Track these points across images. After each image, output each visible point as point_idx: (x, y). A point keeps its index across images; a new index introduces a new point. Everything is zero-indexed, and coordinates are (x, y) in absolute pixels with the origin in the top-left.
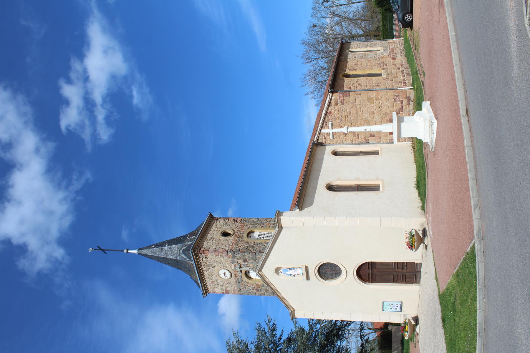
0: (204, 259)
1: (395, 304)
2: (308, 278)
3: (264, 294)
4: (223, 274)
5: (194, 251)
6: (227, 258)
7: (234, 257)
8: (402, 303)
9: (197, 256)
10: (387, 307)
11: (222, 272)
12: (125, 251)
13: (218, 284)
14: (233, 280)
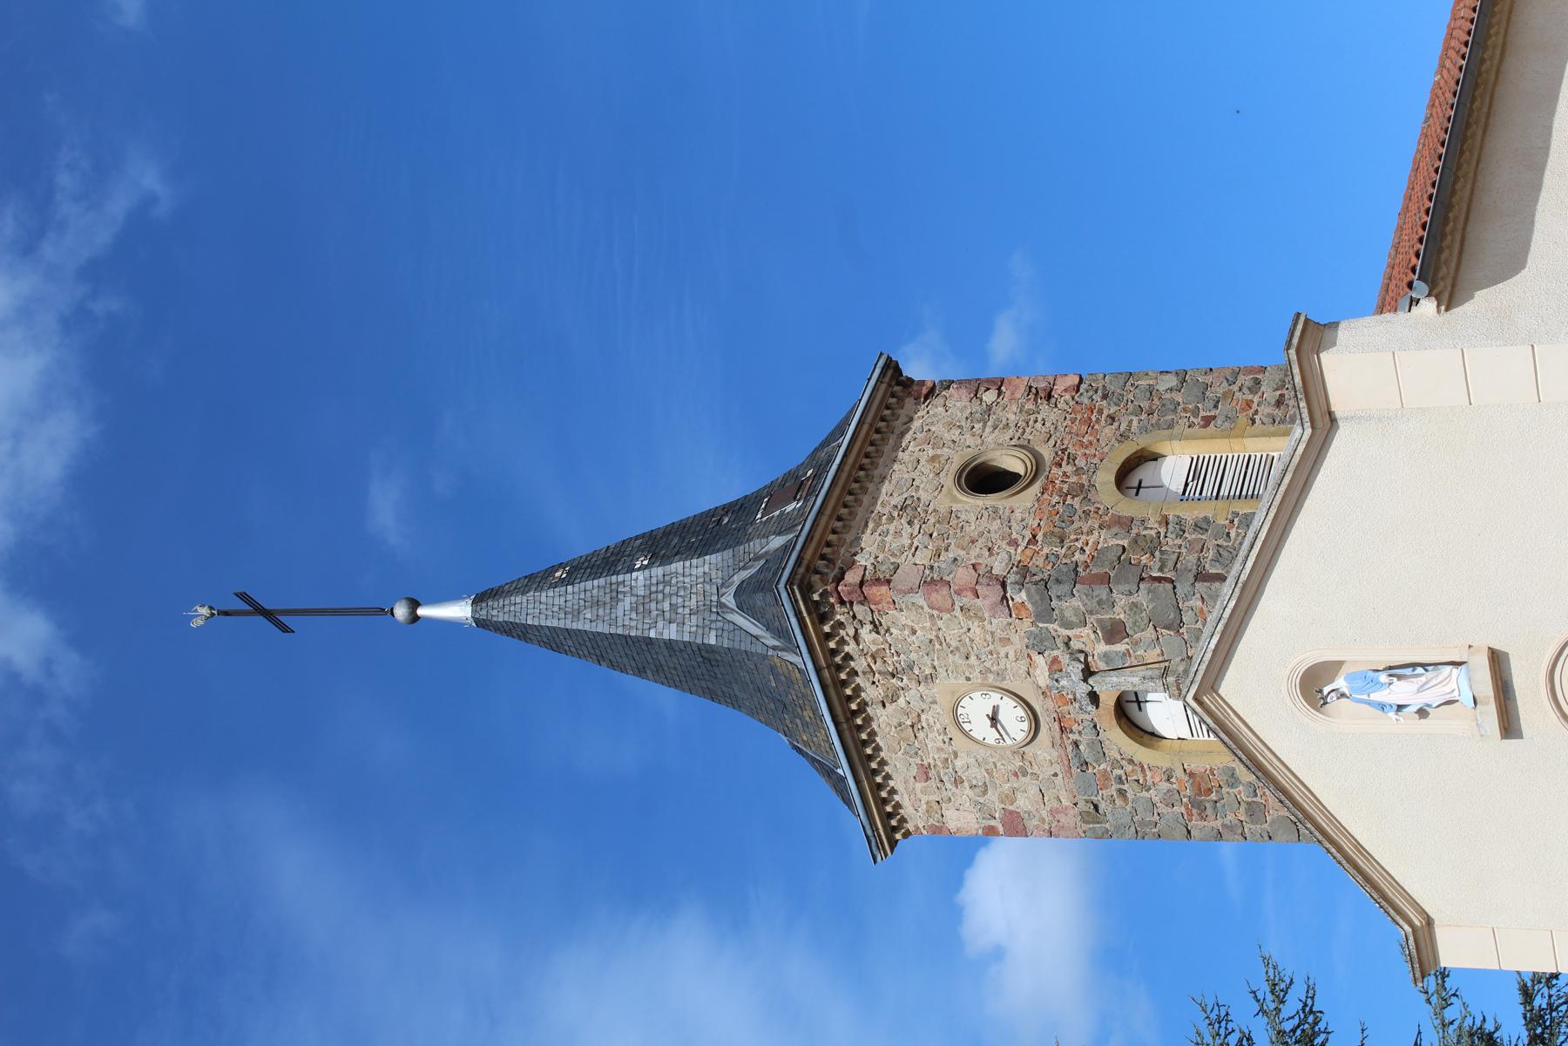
0: (866, 633)
2: (1509, 726)
4: (987, 717)
5: (807, 590)
6: (1000, 621)
7: (1045, 613)
9: (823, 618)
11: (975, 709)
12: (401, 612)
13: (958, 782)
14: (1044, 750)
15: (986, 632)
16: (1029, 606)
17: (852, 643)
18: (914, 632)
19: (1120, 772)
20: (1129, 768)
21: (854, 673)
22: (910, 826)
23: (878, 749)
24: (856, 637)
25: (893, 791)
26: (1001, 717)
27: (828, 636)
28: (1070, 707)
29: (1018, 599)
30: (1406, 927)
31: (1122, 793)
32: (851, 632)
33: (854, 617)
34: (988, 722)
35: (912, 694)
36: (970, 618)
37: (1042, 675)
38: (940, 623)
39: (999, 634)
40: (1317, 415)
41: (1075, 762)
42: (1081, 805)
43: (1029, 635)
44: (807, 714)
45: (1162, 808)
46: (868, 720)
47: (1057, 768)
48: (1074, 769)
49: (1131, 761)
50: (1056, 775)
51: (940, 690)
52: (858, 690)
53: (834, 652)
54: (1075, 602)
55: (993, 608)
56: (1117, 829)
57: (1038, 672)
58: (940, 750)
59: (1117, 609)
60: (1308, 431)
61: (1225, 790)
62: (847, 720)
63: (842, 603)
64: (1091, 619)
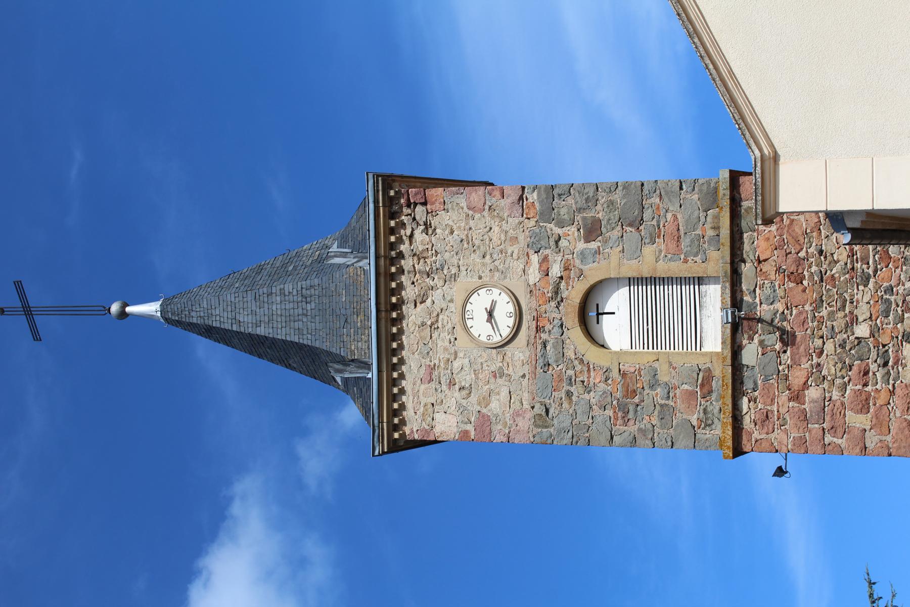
0: (419, 236)
3: (649, 434)
4: (488, 312)
5: (387, 186)
7: (548, 214)
9: (393, 215)
11: (479, 304)
12: (115, 308)
13: (452, 384)
14: (519, 352)
16: (537, 205)
17: (407, 242)
18: (452, 232)
19: (570, 372)
20: (579, 368)
21: (401, 271)
22: (407, 430)
23: (401, 347)
24: (411, 237)
25: (402, 391)
26: (495, 314)
27: (392, 231)
28: (547, 307)
29: (530, 200)
30: (757, 152)
31: (569, 394)
32: (408, 232)
33: (414, 219)
34: (486, 316)
35: (437, 295)
36: (493, 217)
37: (534, 275)
38: (471, 223)
41: (541, 362)
42: (537, 406)
43: (533, 235)
44: (361, 317)
45: (596, 411)
46: (401, 318)
47: (526, 369)
48: (539, 368)
49: (582, 361)
50: (524, 376)
51: (456, 291)
52: (400, 286)
53: (392, 246)
54: (570, 201)
55: (511, 208)
56: (559, 432)
57: (531, 270)
58: (446, 349)
59: (599, 207)
61: (647, 391)
62: (386, 311)
63: (409, 206)
64: (578, 218)
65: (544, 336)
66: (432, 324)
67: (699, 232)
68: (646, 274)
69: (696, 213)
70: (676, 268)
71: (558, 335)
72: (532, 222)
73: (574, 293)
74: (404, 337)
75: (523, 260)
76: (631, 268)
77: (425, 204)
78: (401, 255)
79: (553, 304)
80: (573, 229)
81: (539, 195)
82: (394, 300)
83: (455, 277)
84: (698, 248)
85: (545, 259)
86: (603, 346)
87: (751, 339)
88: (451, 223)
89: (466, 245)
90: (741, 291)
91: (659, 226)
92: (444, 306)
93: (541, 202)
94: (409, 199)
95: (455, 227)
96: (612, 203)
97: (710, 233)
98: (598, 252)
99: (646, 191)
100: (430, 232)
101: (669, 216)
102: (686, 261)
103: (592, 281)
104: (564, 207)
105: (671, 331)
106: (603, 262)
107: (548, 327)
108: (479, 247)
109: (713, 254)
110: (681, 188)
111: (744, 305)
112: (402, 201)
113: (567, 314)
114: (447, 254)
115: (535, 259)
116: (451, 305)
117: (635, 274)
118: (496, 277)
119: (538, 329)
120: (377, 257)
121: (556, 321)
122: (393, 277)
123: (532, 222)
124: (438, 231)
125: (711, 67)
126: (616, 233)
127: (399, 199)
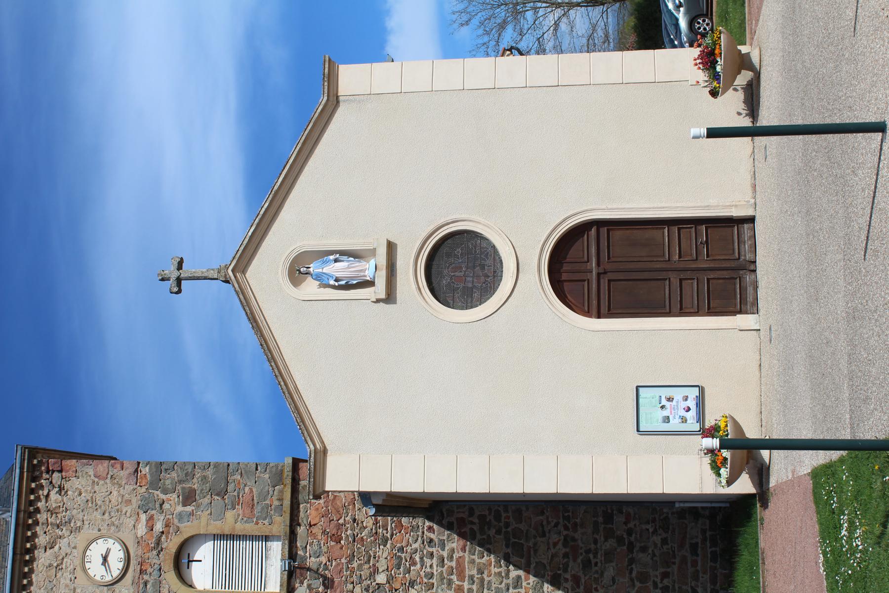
0: (54, 496)
1: (678, 394)
2: (390, 297)
4: (103, 558)
5: (32, 456)
7: (155, 484)
8: (702, 390)
9: (34, 479)
10: (652, 419)
11: (96, 550)
15: (120, 495)
16: (148, 476)
17: (44, 501)
18: (80, 494)
21: (36, 523)
24: (47, 496)
26: (109, 559)
27: (33, 491)
28: (150, 554)
29: (143, 472)
30: (312, 446)
32: (45, 493)
33: (51, 482)
35: (63, 543)
36: (114, 484)
37: (142, 530)
39: (127, 497)
40: (331, 94)
43: (143, 499)
46: (32, 560)
51: (80, 540)
52: (35, 535)
53: (31, 503)
54: (174, 474)
58: (67, 586)
59: (195, 480)
60: (326, 98)
63: (48, 472)
64: (179, 488)
65: (146, 577)
66: (58, 565)
67: (268, 502)
68: (227, 532)
69: (267, 488)
70: (250, 528)
71: (156, 577)
72: (144, 489)
73: (171, 545)
74: (33, 576)
75: (134, 518)
76: (216, 527)
77: (61, 471)
78: (38, 511)
79: (155, 552)
80: (175, 496)
81: (150, 469)
82: (28, 545)
83: (79, 529)
84: (266, 514)
85: (151, 518)
86: (191, 586)
87: (302, 583)
88: (80, 487)
89: (90, 505)
90: (296, 547)
91: (238, 496)
92: (69, 551)
93: (151, 475)
94: (48, 467)
95: (83, 490)
96: (204, 478)
97: (276, 503)
98: (192, 514)
99: (231, 470)
100: (63, 493)
101: (247, 489)
102: (257, 523)
103: (186, 536)
104: (169, 479)
105: (243, 575)
106: (195, 522)
107: (149, 570)
108: (100, 507)
109: (277, 519)
110: (257, 469)
111: (298, 557)
112: (43, 468)
113: (165, 560)
114: (75, 511)
115: (143, 517)
116: (74, 550)
117: (219, 532)
118: (112, 530)
119: (141, 572)
120: (18, 511)
121: (156, 566)
122: (29, 527)
123: (144, 489)
124: (69, 493)
125: (282, 383)
126: (206, 500)
127: (41, 466)
